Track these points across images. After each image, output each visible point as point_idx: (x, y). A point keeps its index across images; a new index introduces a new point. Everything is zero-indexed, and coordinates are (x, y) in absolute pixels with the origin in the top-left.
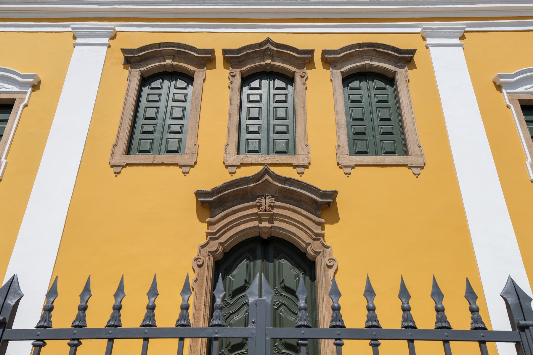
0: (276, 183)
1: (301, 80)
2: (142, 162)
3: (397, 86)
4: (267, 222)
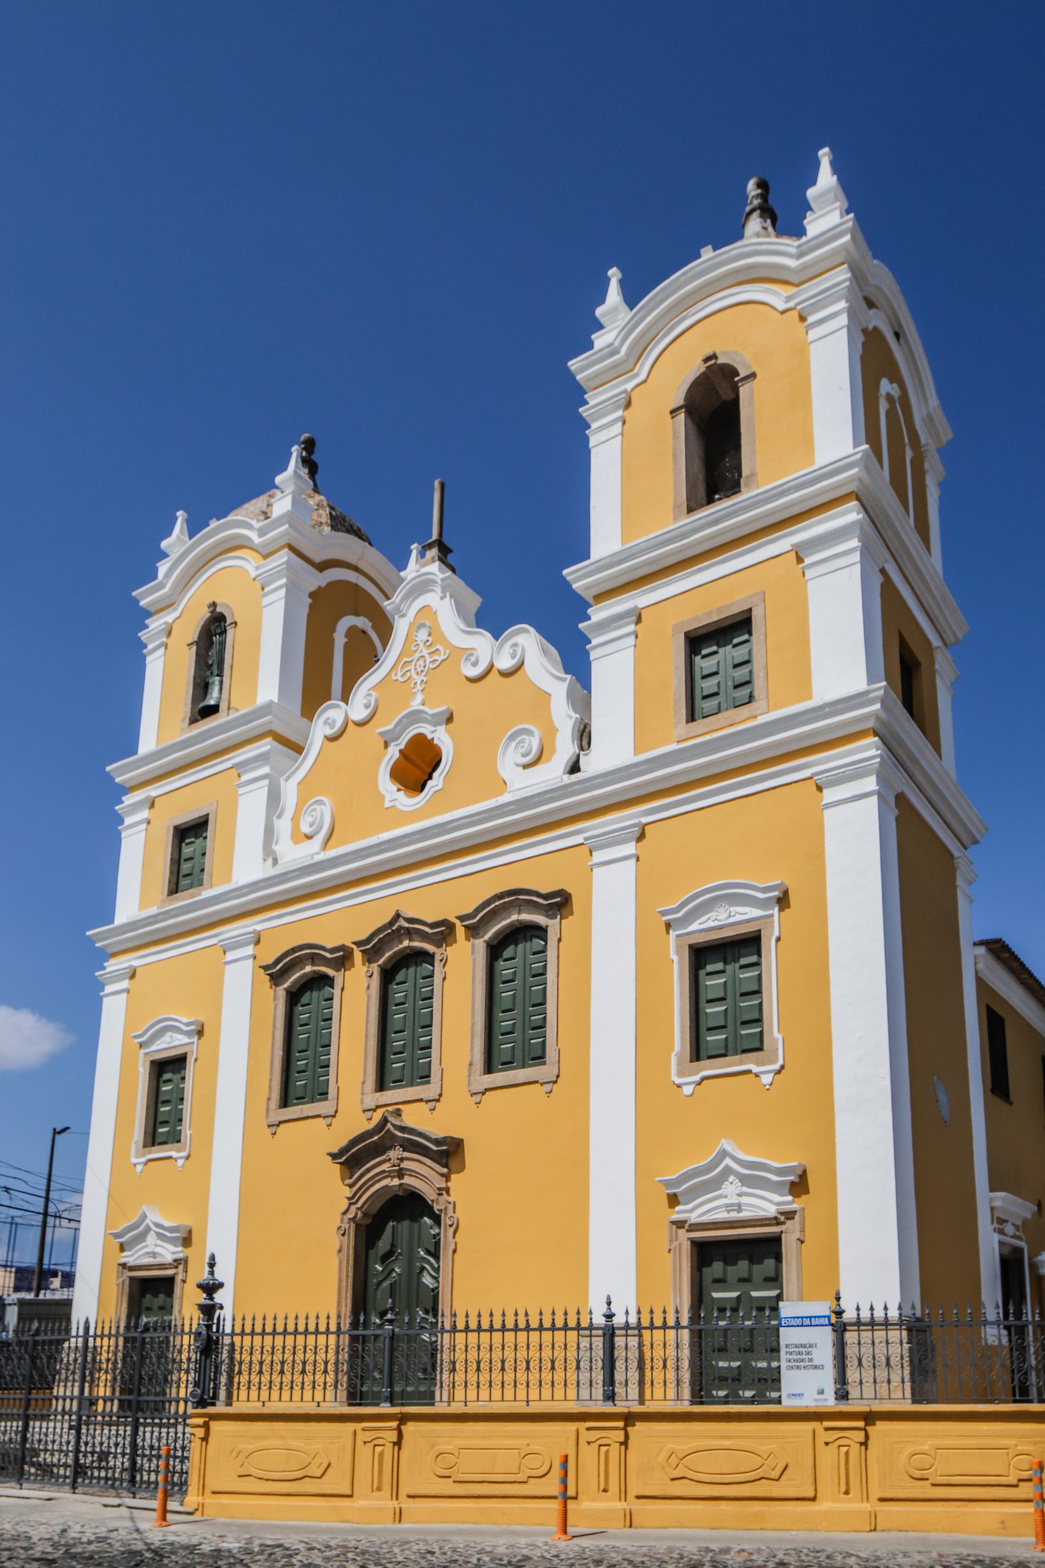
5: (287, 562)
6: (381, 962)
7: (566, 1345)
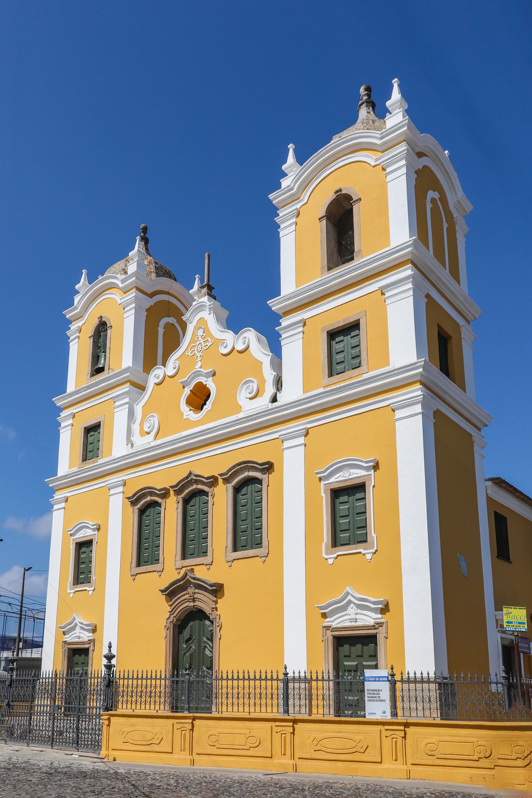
5: (135, 296)
7: (266, 687)
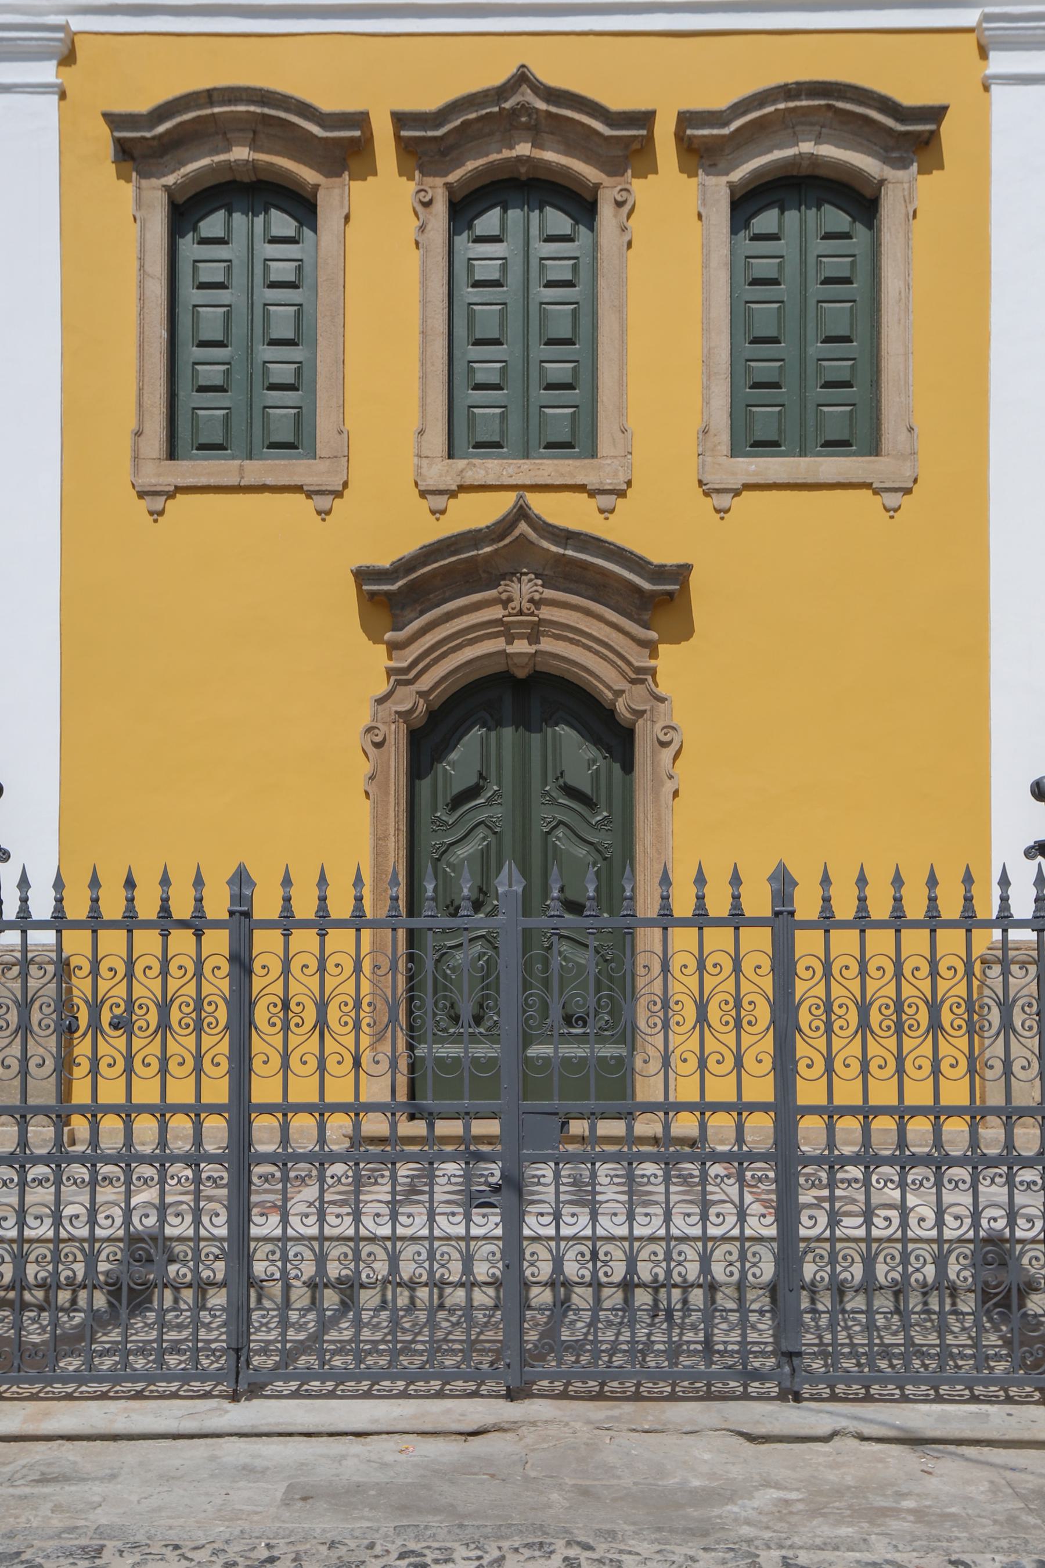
0: (545, 544)
1: (615, 216)
2: (213, 481)
3: (879, 230)
4: (526, 641)
6: (453, 177)
